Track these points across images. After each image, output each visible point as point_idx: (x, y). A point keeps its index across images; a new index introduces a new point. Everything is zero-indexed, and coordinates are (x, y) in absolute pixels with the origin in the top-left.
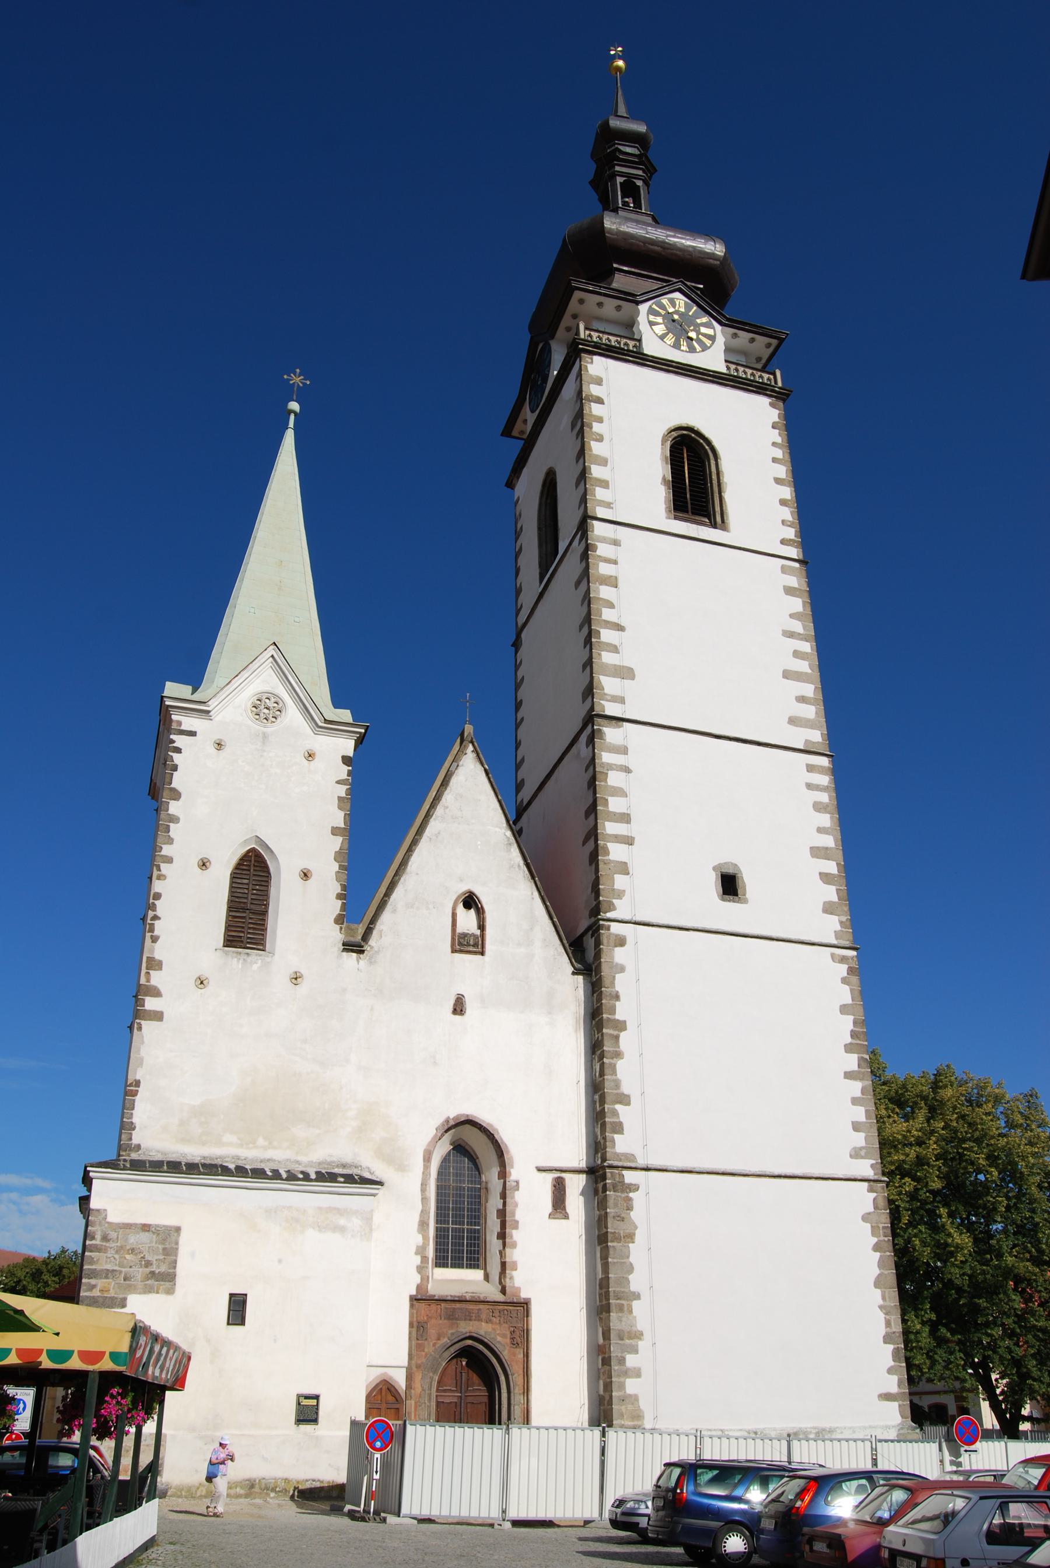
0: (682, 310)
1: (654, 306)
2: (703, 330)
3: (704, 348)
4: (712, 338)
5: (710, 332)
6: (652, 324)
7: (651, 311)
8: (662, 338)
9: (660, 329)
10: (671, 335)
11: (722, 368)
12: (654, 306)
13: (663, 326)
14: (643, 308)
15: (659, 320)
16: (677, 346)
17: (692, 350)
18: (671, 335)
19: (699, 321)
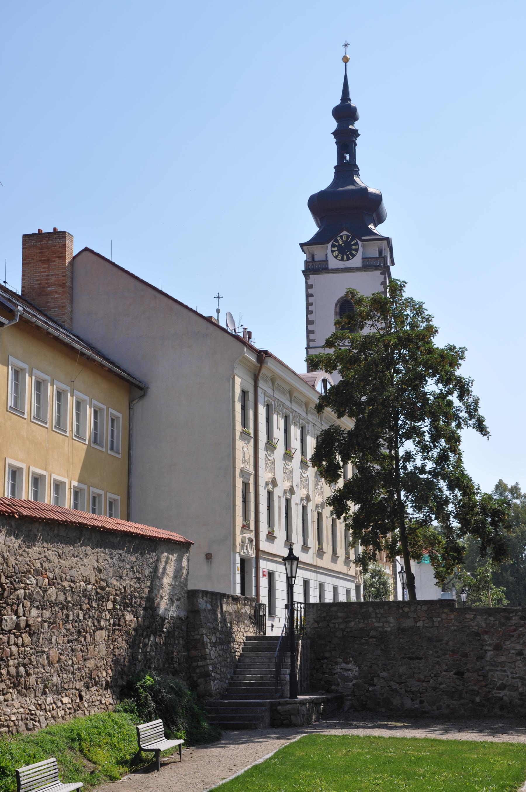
0: (345, 240)
1: (334, 243)
2: (354, 247)
3: (353, 256)
4: (357, 250)
5: (356, 247)
6: (333, 252)
7: (333, 246)
8: (336, 257)
9: (336, 253)
10: (340, 255)
11: (360, 265)
12: (334, 243)
13: (337, 252)
14: (330, 245)
15: (336, 249)
16: (342, 260)
17: (348, 259)
18: (340, 255)
19: (352, 243)
